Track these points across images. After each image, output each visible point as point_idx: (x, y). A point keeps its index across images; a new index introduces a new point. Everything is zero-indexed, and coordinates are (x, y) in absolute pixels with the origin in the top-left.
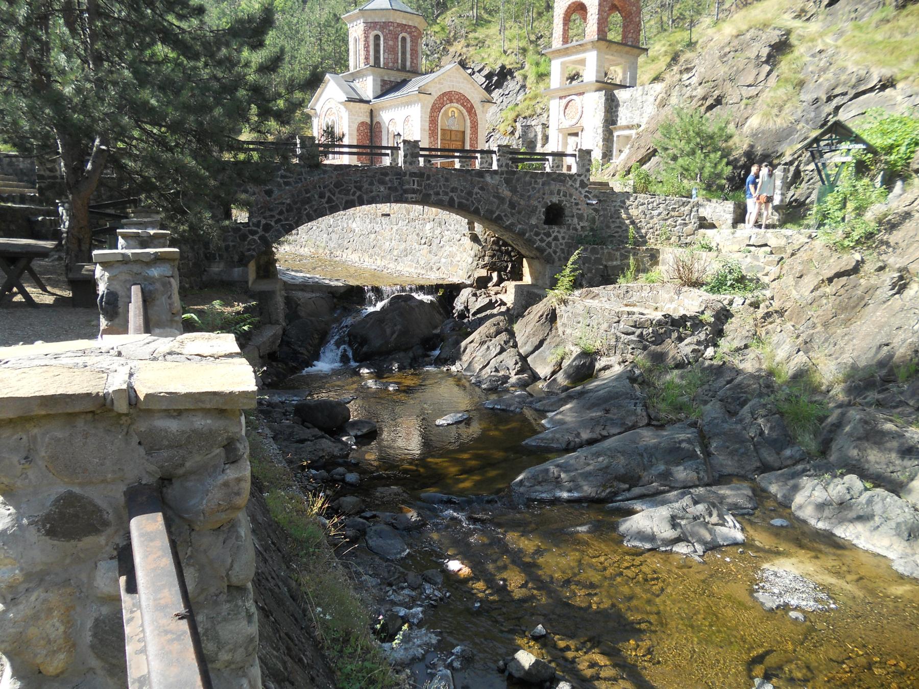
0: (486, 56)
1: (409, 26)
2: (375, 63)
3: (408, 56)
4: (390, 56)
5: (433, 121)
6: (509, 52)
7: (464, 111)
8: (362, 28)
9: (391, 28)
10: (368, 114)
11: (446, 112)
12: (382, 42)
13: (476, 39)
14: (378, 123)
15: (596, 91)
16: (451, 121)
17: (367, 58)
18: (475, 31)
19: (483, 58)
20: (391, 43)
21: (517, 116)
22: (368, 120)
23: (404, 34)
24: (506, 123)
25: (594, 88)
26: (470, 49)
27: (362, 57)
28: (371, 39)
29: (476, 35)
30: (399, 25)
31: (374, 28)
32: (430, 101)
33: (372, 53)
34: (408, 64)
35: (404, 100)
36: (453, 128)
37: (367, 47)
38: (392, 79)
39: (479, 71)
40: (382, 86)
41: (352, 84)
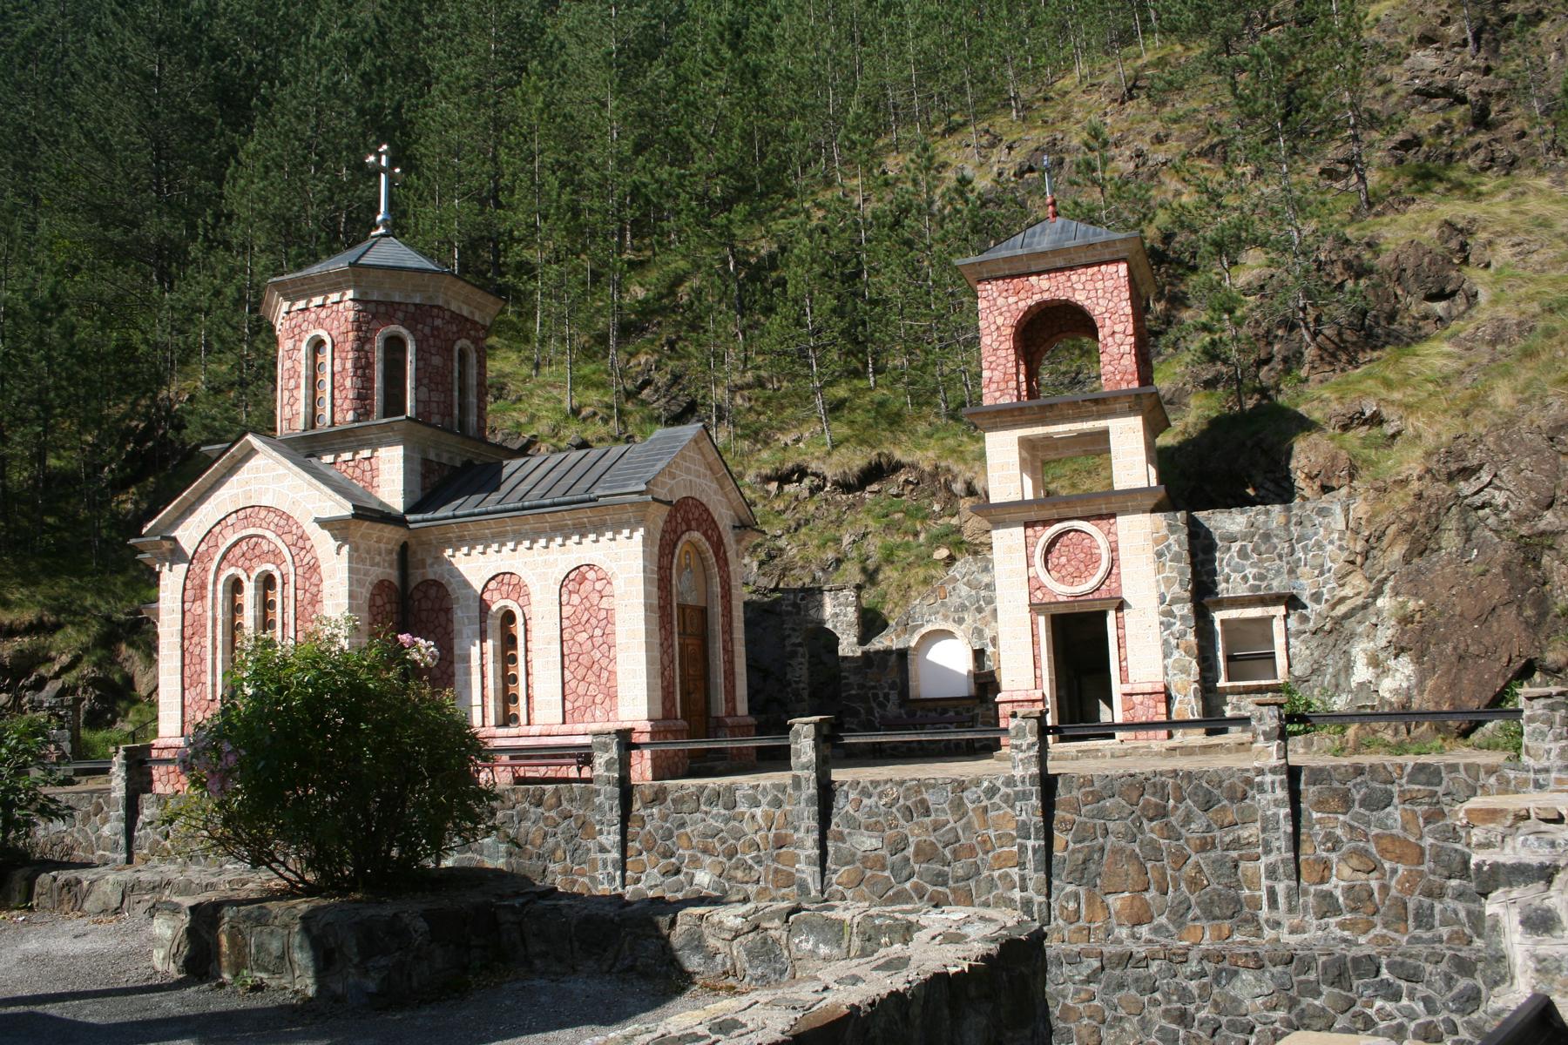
4: (435, 397)
6: (586, 412)
8: (351, 315)
9: (438, 322)
10: (395, 556)
12: (410, 357)
15: (1153, 511)
20: (436, 360)
22: (393, 574)
25: (1151, 502)
28: (378, 343)
30: (457, 318)
31: (390, 319)
37: (363, 368)
38: (444, 459)
40: (424, 476)
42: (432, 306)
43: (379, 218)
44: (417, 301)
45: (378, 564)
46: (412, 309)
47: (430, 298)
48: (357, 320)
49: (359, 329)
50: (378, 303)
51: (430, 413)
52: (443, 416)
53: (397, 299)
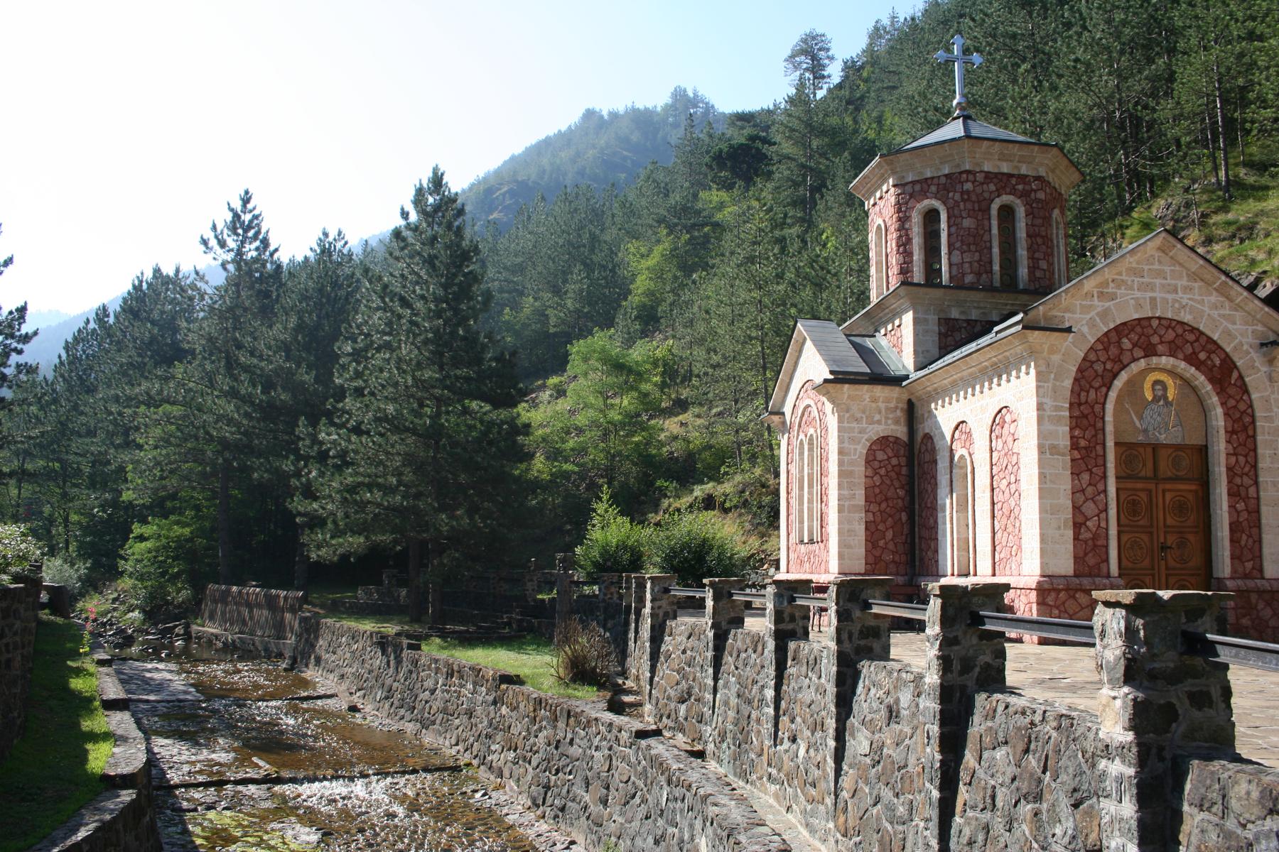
0: (1261, 256)
1: (1022, 178)
2: (927, 278)
3: (1022, 253)
7: (1201, 379)
8: (893, 200)
9: (968, 186)
11: (1133, 387)
12: (944, 225)
13: (1229, 223)
14: (928, 437)
16: (1152, 417)
17: (905, 270)
18: (1225, 209)
19: (1253, 262)
20: (967, 223)
22: (901, 431)
23: (1006, 199)
26: (1216, 247)
27: (894, 270)
29: (1230, 216)
31: (924, 194)
33: (918, 256)
34: (1023, 272)
35: (990, 356)
36: (1163, 438)
37: (904, 245)
41: (868, 342)
42: (961, 173)
43: (955, 102)
44: (947, 172)
45: (879, 422)
46: (943, 180)
47: (958, 166)
48: (898, 203)
49: (899, 211)
50: (913, 183)
51: (964, 275)
52: (979, 274)
53: (929, 175)
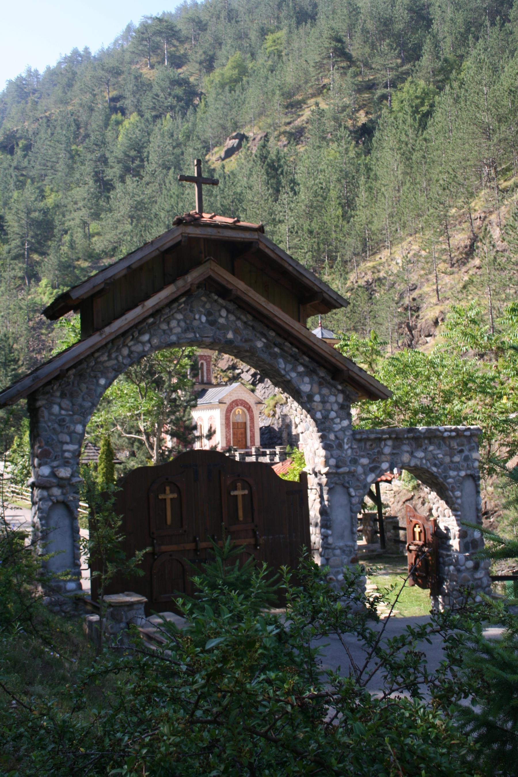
3: (205, 374)
5: (227, 418)
11: (235, 412)
21: (276, 403)
24: (269, 408)
32: (225, 406)
34: (205, 379)
39: (247, 372)
